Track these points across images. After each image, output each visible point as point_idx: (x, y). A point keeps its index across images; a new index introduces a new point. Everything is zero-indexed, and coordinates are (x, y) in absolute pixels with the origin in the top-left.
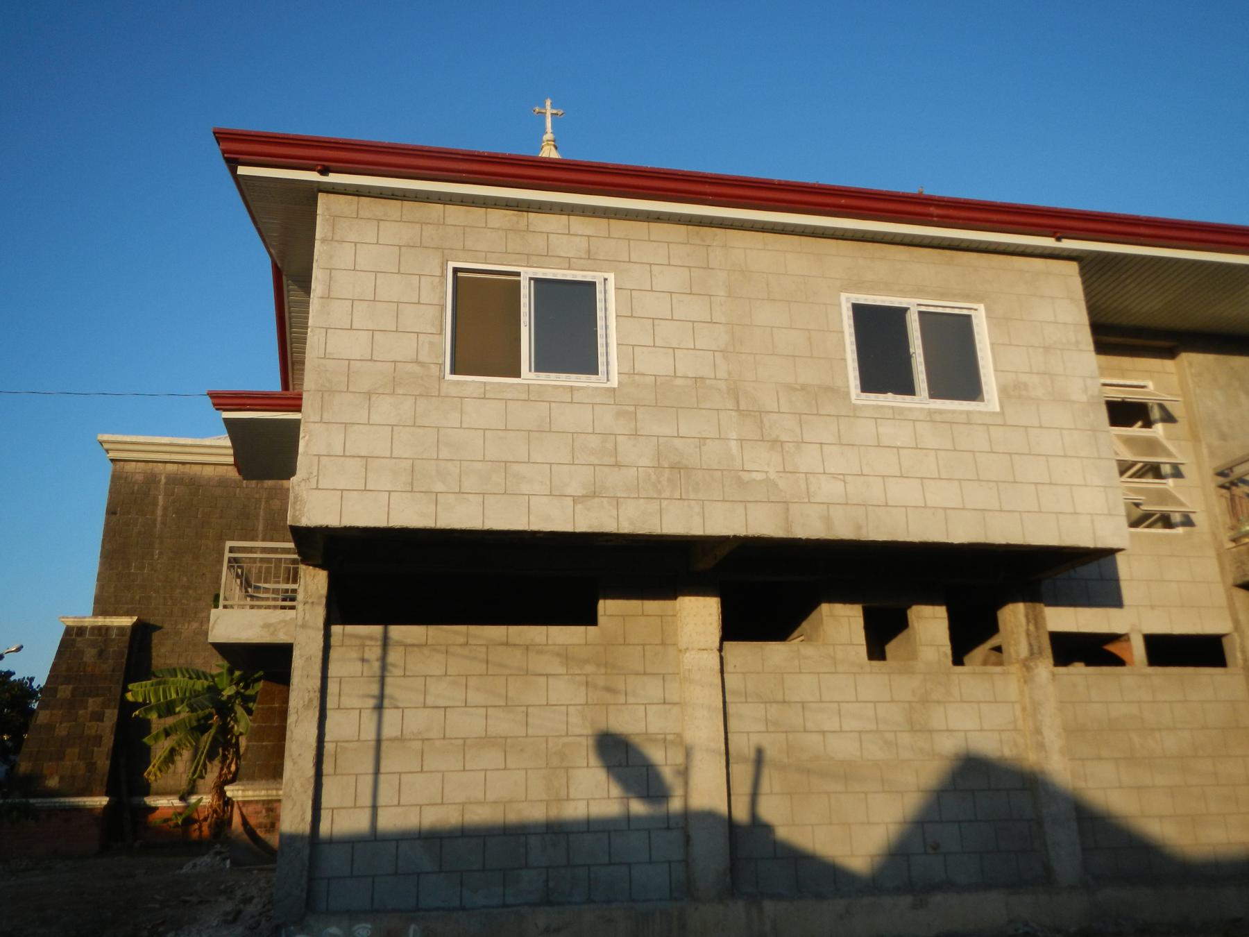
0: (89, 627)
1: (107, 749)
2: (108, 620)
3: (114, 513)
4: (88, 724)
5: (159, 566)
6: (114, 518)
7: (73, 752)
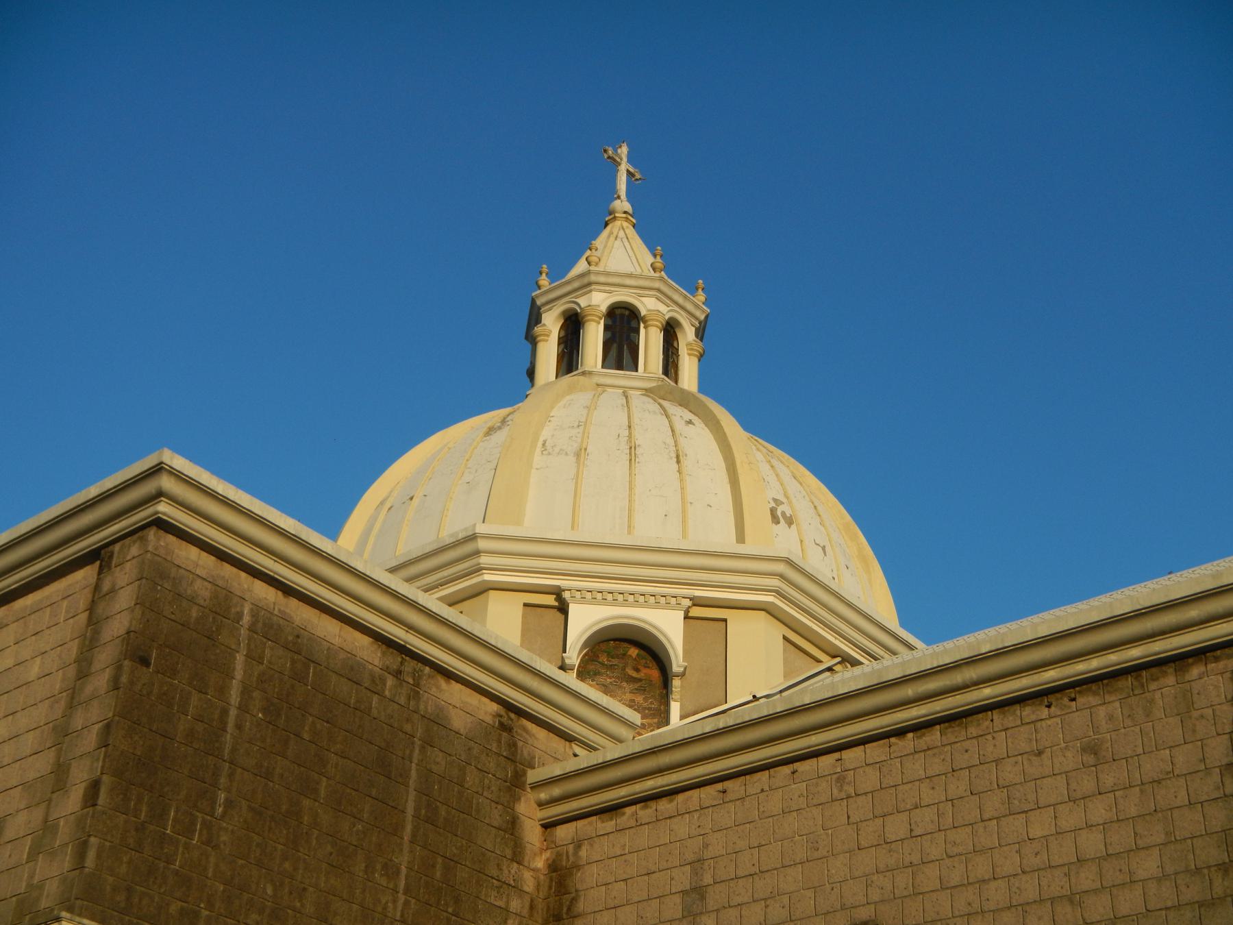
3: (145, 662)
5: (224, 838)
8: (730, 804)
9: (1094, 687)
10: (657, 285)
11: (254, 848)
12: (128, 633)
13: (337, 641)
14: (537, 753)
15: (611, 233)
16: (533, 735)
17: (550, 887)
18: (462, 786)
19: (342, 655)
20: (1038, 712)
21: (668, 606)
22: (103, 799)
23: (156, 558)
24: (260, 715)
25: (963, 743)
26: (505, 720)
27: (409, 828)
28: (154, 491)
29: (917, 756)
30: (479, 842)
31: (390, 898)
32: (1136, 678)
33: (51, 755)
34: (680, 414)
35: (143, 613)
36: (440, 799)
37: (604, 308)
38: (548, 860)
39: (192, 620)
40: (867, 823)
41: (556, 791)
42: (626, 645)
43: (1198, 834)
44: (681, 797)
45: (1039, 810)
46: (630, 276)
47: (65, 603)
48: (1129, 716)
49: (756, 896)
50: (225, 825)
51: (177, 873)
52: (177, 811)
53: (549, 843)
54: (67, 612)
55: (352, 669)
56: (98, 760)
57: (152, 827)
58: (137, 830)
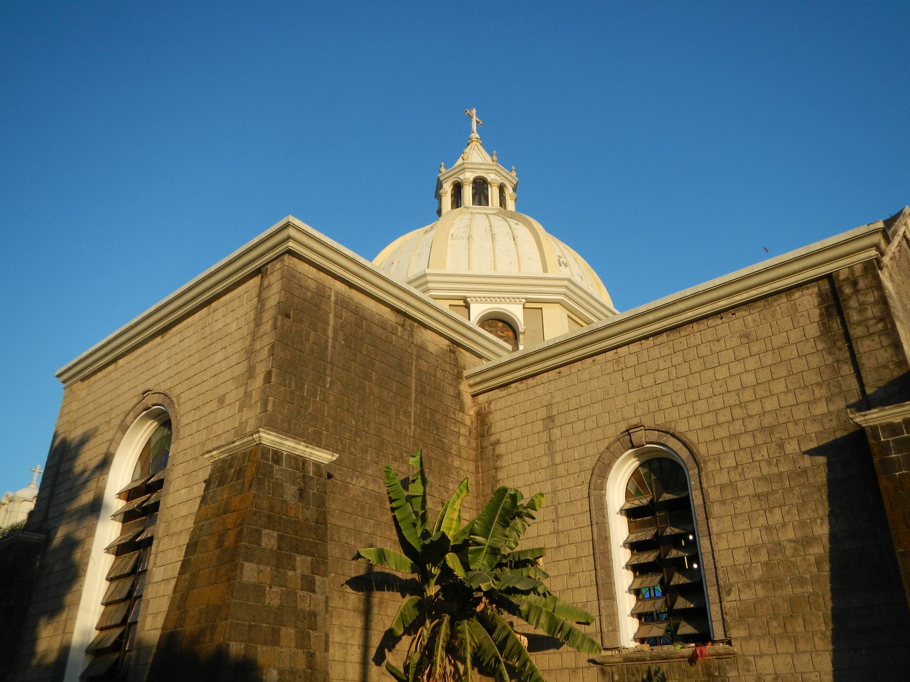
0: (285, 453)
1: (324, 635)
2: (308, 450)
3: (288, 316)
4: (300, 593)
5: (331, 398)
6: (289, 322)
7: (288, 633)
8: (563, 378)
9: (744, 307)
10: (494, 168)
11: (345, 403)
12: (279, 303)
13: (374, 309)
14: (467, 364)
15: (471, 147)
16: (464, 355)
17: (478, 423)
18: (435, 377)
19: (378, 316)
20: (716, 322)
21: (515, 303)
22: (273, 379)
23: (290, 268)
24: (343, 342)
25: (679, 339)
26: (452, 348)
27: (413, 396)
28: (286, 237)
29: (655, 347)
30: (445, 403)
31: (408, 427)
32: (766, 301)
33: (246, 363)
34: (512, 222)
35: (285, 294)
36: (426, 383)
37: (471, 179)
38: (475, 411)
39: (308, 298)
40: (632, 380)
41: (478, 379)
42: (497, 322)
43: (805, 370)
44: (538, 377)
45: (720, 367)
46: (482, 164)
47: (246, 295)
48: (764, 319)
49: (580, 418)
50: (330, 392)
51: (310, 414)
52: (308, 386)
53: (475, 403)
54: (247, 299)
55: (382, 323)
56: (269, 361)
57: (297, 393)
58: (290, 394)
